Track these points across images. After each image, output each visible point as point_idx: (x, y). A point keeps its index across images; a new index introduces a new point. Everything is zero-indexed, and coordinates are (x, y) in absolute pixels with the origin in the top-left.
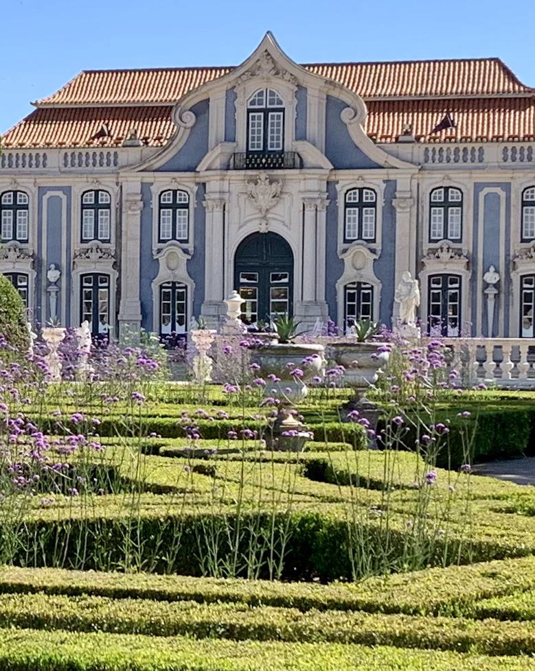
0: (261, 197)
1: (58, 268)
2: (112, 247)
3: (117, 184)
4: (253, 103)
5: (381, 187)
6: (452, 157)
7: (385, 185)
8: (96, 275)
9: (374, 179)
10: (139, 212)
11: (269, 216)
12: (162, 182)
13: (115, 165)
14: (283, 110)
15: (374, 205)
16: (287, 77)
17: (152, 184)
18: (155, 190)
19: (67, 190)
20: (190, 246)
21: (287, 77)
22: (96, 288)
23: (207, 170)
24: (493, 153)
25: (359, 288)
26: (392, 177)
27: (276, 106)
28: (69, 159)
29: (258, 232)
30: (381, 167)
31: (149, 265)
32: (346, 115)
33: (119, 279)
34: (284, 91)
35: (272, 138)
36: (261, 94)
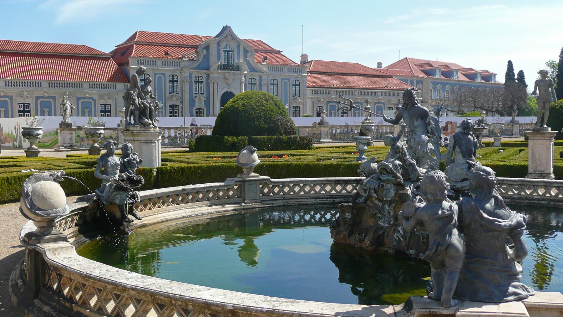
0: (230, 80)
1: (162, 103)
2: (179, 95)
3: (181, 73)
4: (224, 48)
5: (258, 78)
6: (277, 69)
7: (259, 78)
8: (173, 105)
9: (256, 76)
10: (188, 83)
11: (231, 86)
12: (196, 73)
13: (179, 66)
14: (233, 51)
15: (255, 84)
16: (235, 40)
17: (192, 74)
18: (193, 76)
19: (164, 74)
20: (205, 95)
21: (235, 40)
22: (173, 110)
23: (213, 70)
24: (286, 69)
25: (199, 110)
26: (261, 75)
27: (230, 50)
28: (164, 63)
29: (227, 92)
30: (258, 72)
31: (192, 102)
32: (249, 54)
33: (182, 107)
34: (233, 45)
35: (226, 61)
36: (226, 46)
